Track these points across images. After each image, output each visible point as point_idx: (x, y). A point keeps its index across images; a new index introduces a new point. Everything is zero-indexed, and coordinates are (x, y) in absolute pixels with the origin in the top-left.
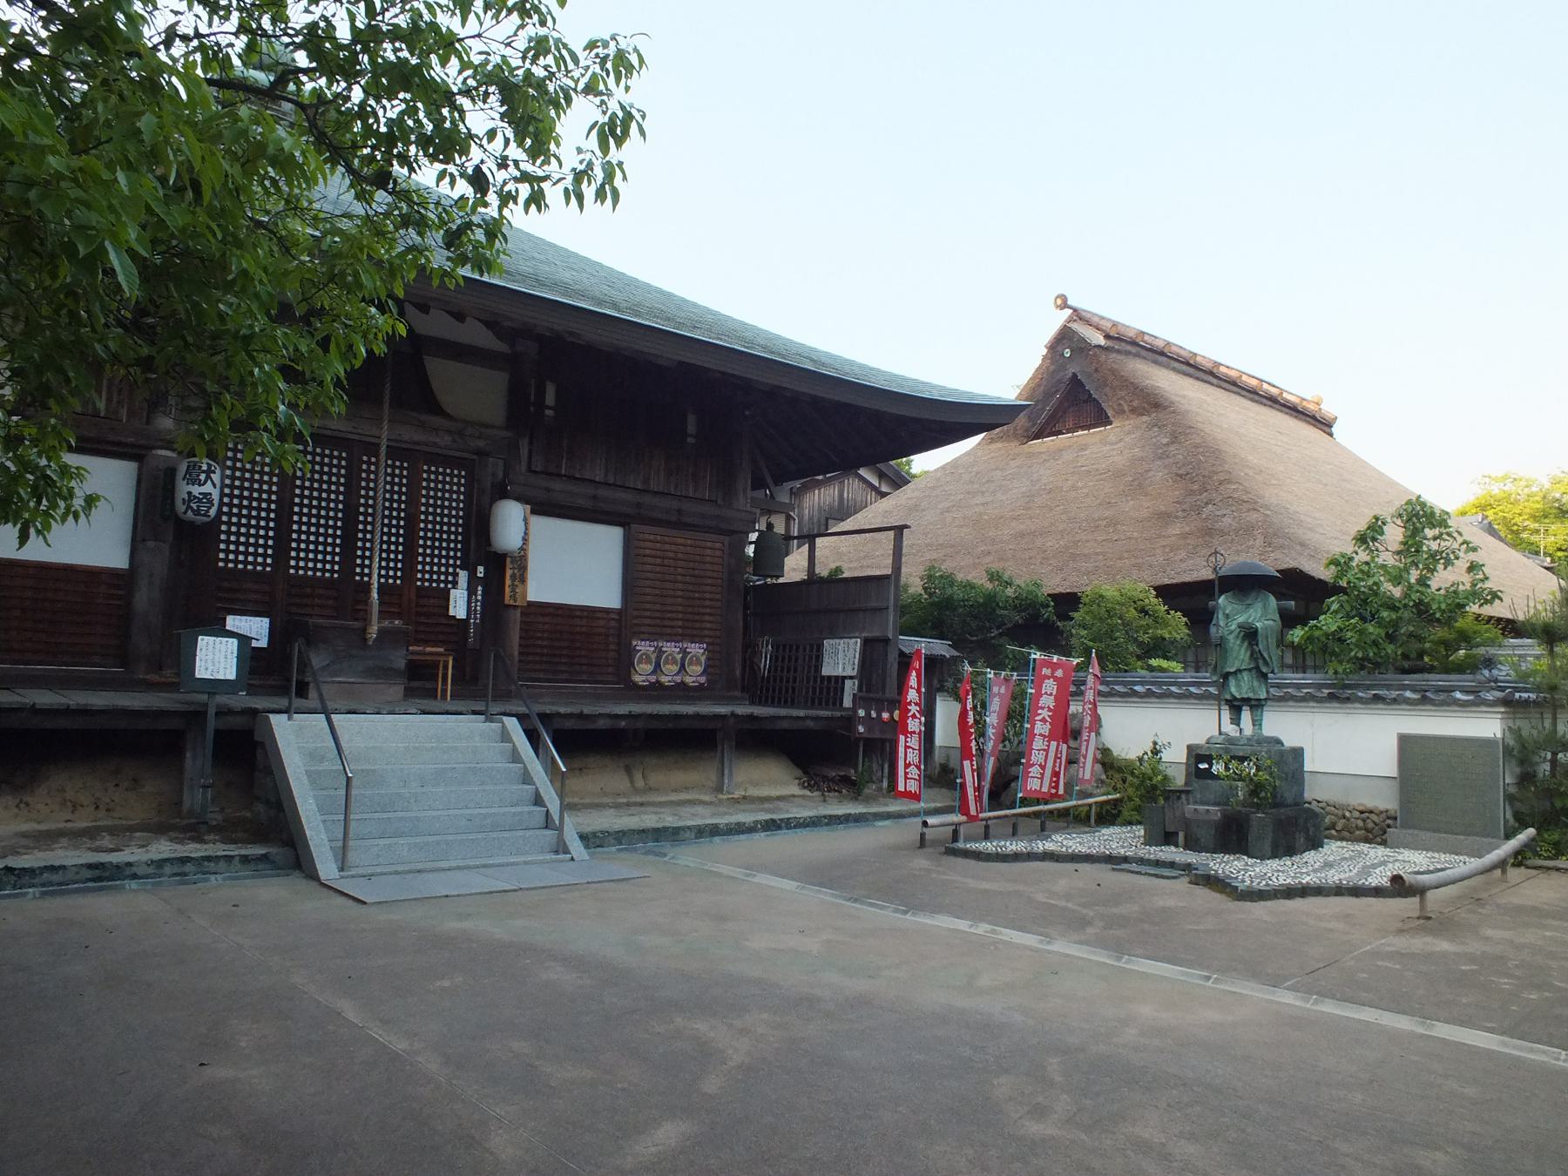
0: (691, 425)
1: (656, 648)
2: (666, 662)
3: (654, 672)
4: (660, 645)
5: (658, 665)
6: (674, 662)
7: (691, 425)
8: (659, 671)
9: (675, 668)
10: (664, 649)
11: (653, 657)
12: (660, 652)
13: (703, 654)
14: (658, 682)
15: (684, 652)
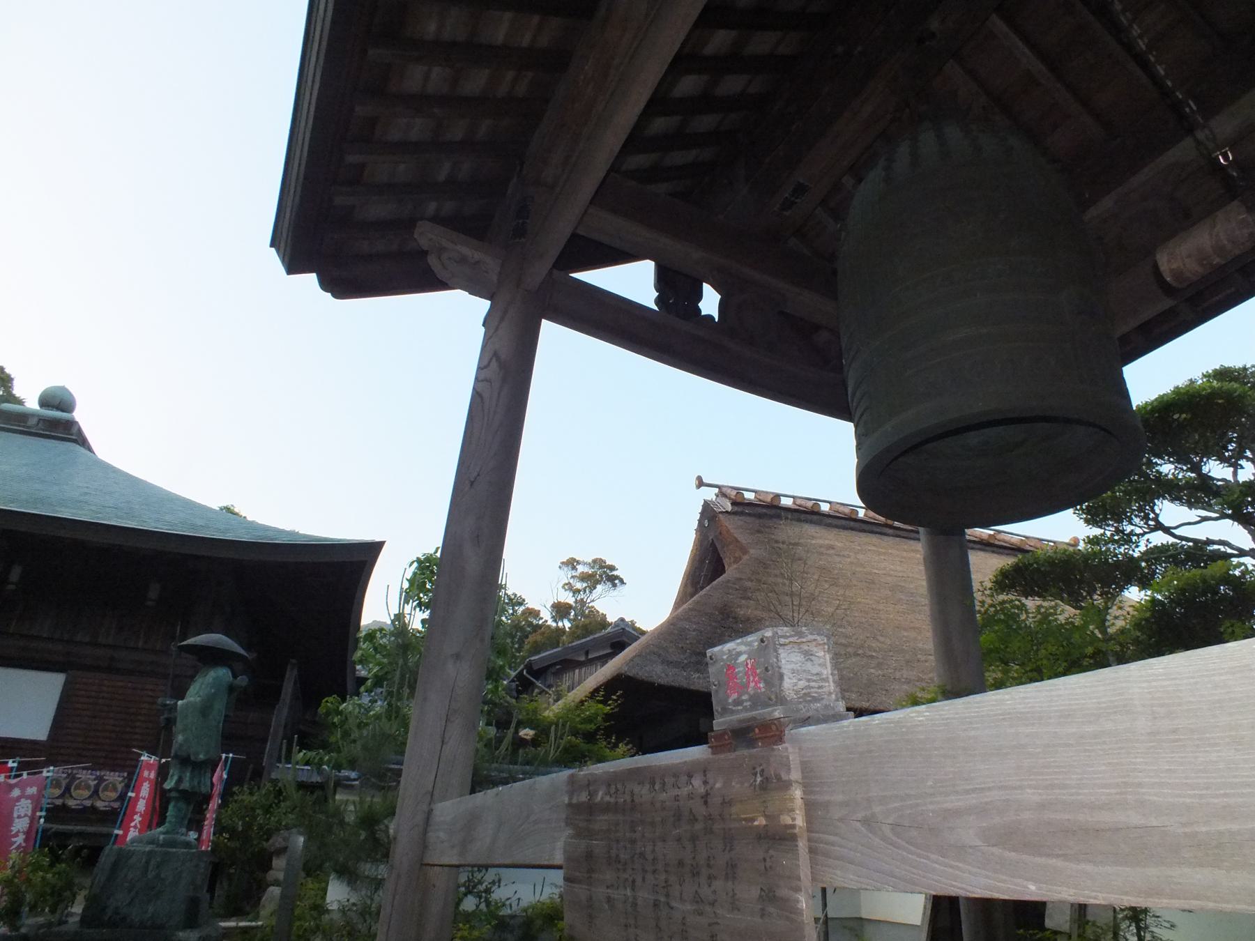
0: (154, 592)
1: (69, 775)
2: (77, 788)
3: (62, 796)
4: (102, 774)
5: (68, 789)
6: (88, 787)
7: (154, 592)
8: (67, 795)
9: (87, 793)
10: (78, 776)
11: (64, 784)
12: (72, 778)
13: (122, 781)
14: (64, 805)
15: (100, 780)
